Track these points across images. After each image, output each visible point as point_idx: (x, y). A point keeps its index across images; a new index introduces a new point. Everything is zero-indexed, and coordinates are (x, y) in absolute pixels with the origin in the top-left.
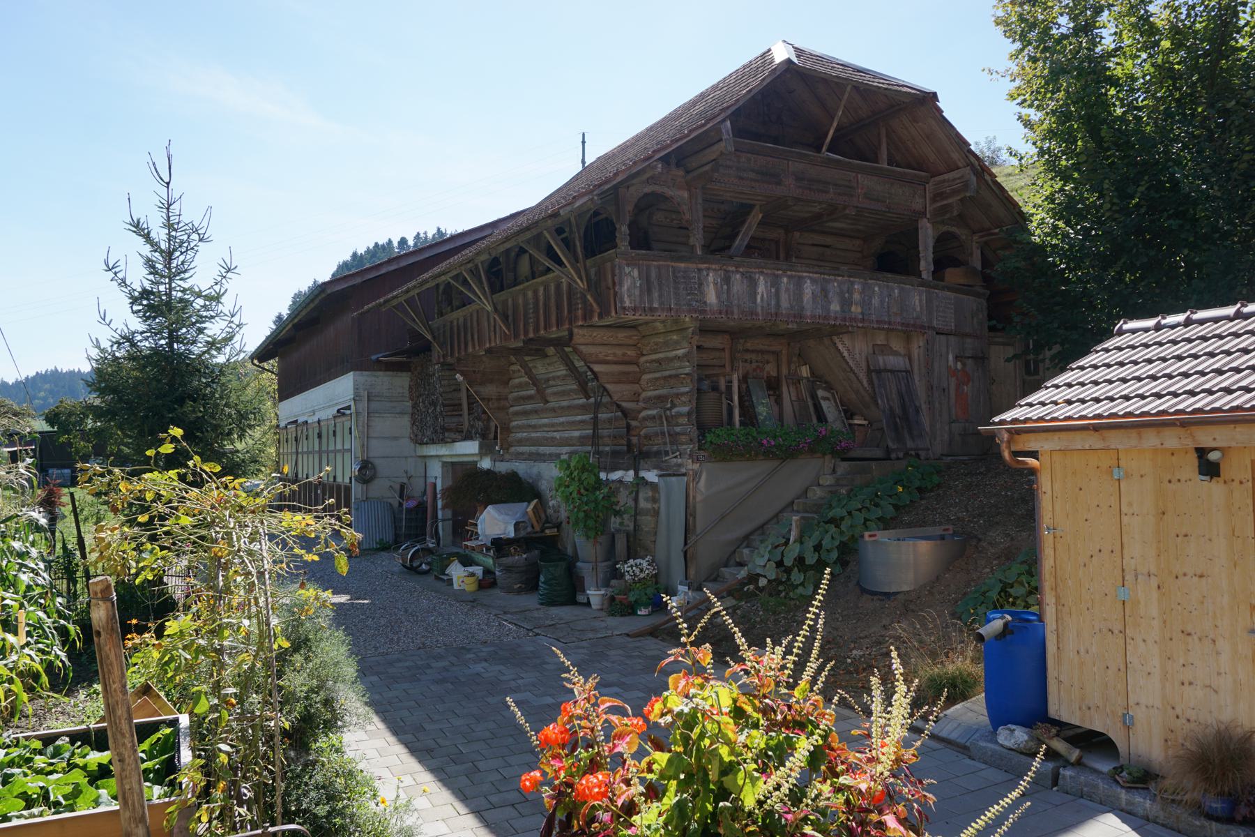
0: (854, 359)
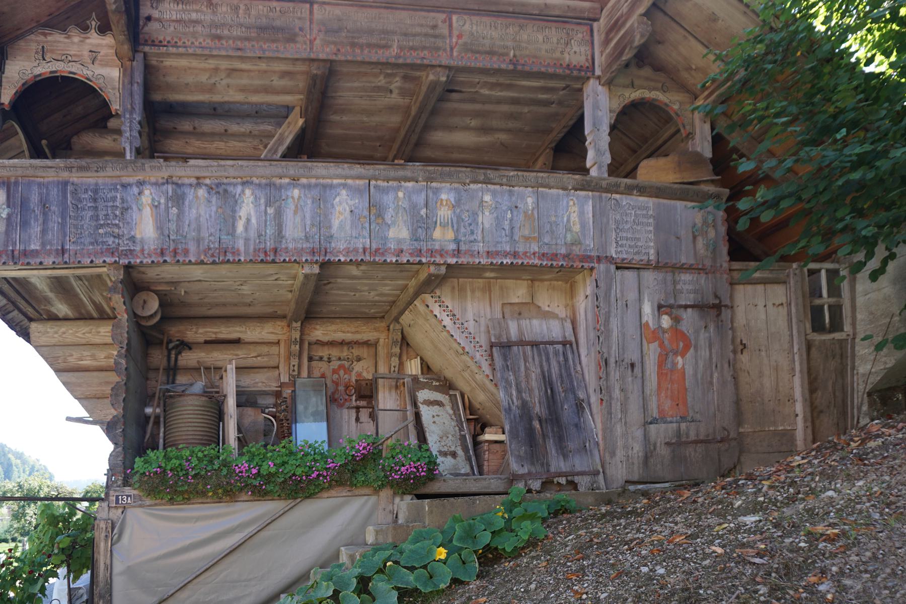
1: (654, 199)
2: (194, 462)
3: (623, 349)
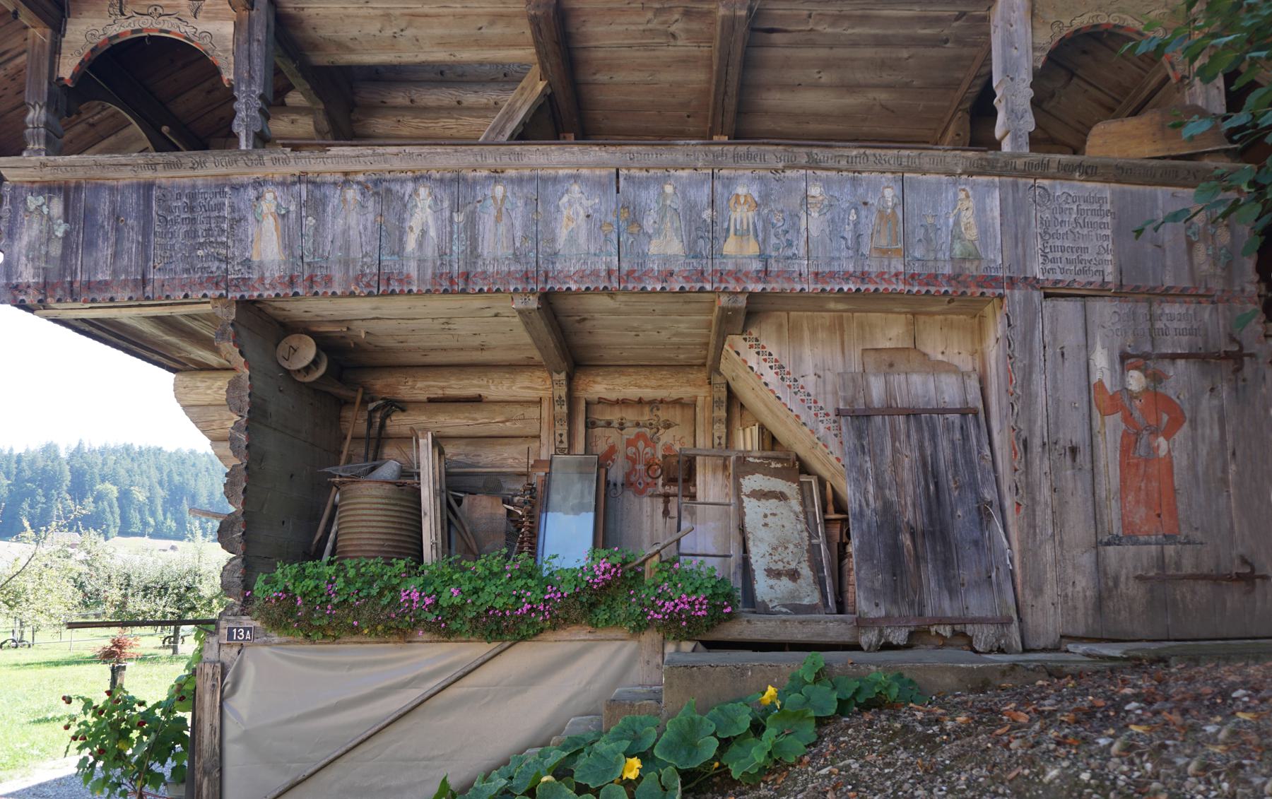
0: (796, 386)
1: (1114, 185)
2: (340, 583)
3: (1056, 424)
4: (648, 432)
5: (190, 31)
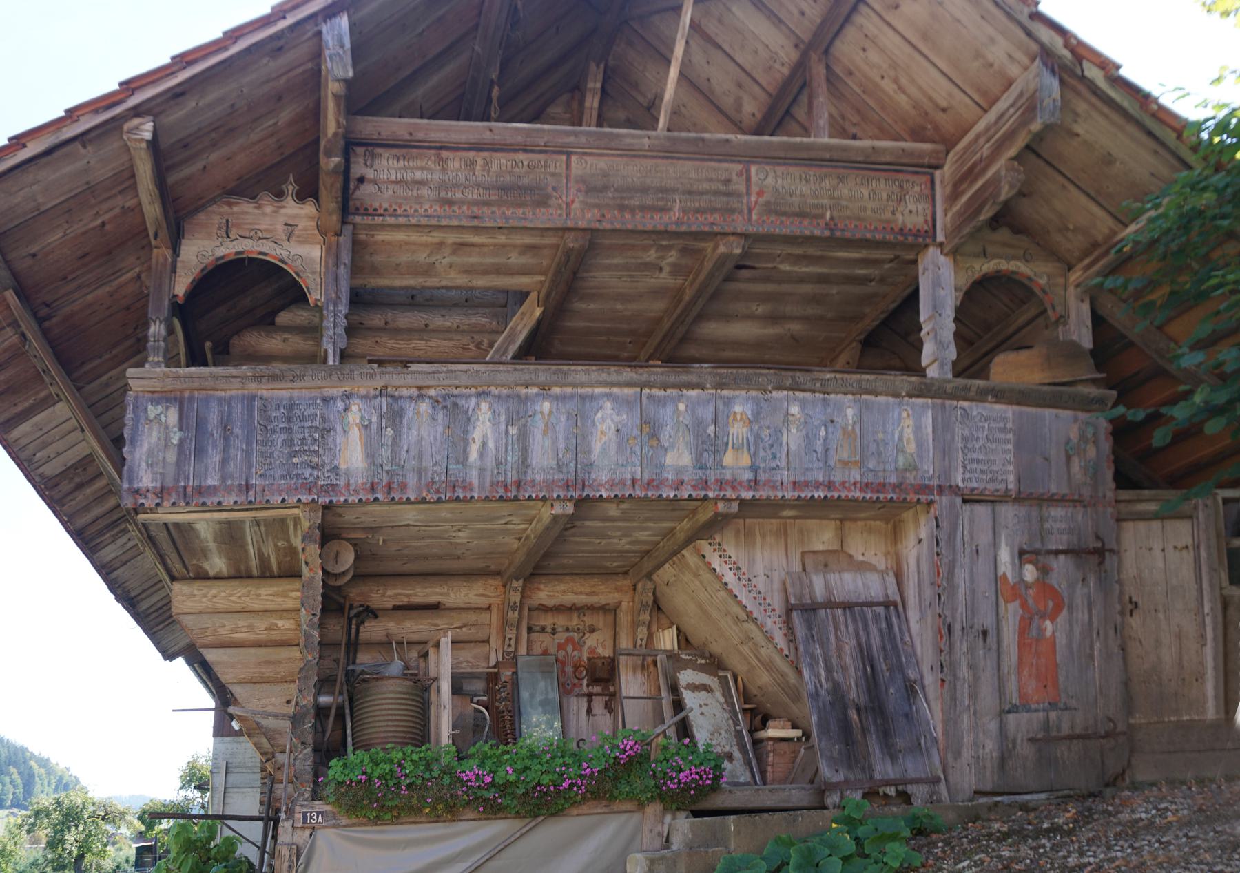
0: (750, 586)
1: (1015, 408)
3: (973, 611)
4: (576, 636)
5: (285, 253)
